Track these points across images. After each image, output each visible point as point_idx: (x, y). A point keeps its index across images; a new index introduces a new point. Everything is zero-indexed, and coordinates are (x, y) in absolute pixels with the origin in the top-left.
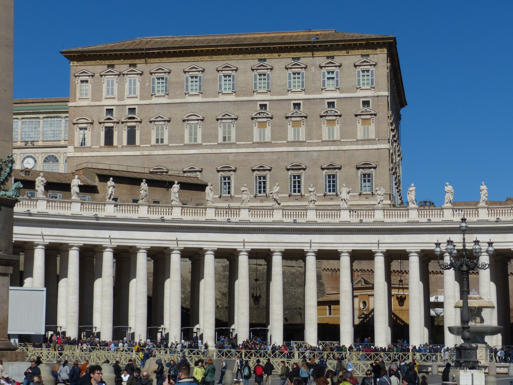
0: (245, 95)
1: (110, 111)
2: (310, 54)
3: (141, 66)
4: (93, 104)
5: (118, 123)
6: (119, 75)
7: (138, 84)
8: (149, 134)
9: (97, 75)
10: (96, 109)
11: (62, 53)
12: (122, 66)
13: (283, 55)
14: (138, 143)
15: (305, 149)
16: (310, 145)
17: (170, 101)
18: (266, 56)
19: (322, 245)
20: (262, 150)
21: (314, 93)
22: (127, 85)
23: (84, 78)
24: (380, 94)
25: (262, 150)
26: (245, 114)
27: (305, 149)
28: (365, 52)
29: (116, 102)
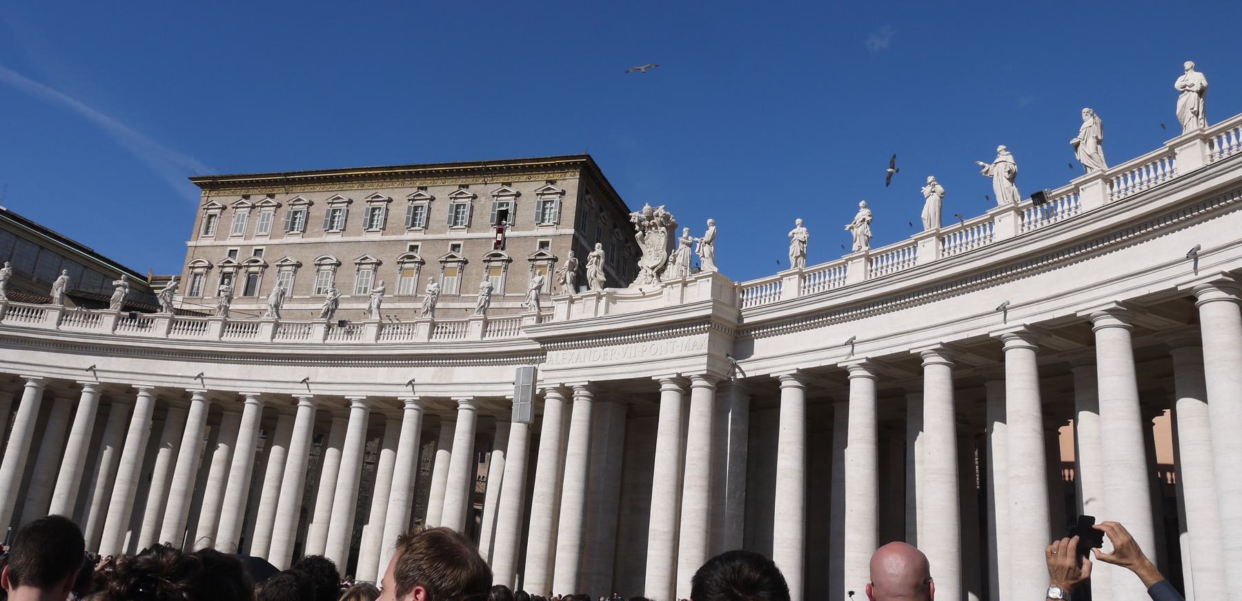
0: (393, 234)
1: (232, 253)
2: (481, 180)
3: (281, 197)
4: (216, 243)
5: (239, 267)
6: (253, 207)
7: (272, 218)
8: (272, 282)
9: (229, 208)
10: (218, 250)
11: (192, 179)
12: (258, 197)
13: (448, 182)
14: (256, 294)
15: (457, 305)
16: (466, 300)
17: (304, 240)
18: (427, 183)
19: (218, 382)
20: (403, 305)
21: (479, 230)
22: (258, 221)
23: (211, 212)
24: (564, 231)
25: (403, 305)
26: (390, 260)
27: (457, 305)
28: (552, 177)
29: (241, 241)
